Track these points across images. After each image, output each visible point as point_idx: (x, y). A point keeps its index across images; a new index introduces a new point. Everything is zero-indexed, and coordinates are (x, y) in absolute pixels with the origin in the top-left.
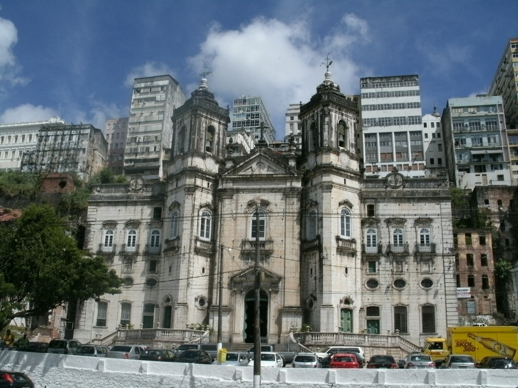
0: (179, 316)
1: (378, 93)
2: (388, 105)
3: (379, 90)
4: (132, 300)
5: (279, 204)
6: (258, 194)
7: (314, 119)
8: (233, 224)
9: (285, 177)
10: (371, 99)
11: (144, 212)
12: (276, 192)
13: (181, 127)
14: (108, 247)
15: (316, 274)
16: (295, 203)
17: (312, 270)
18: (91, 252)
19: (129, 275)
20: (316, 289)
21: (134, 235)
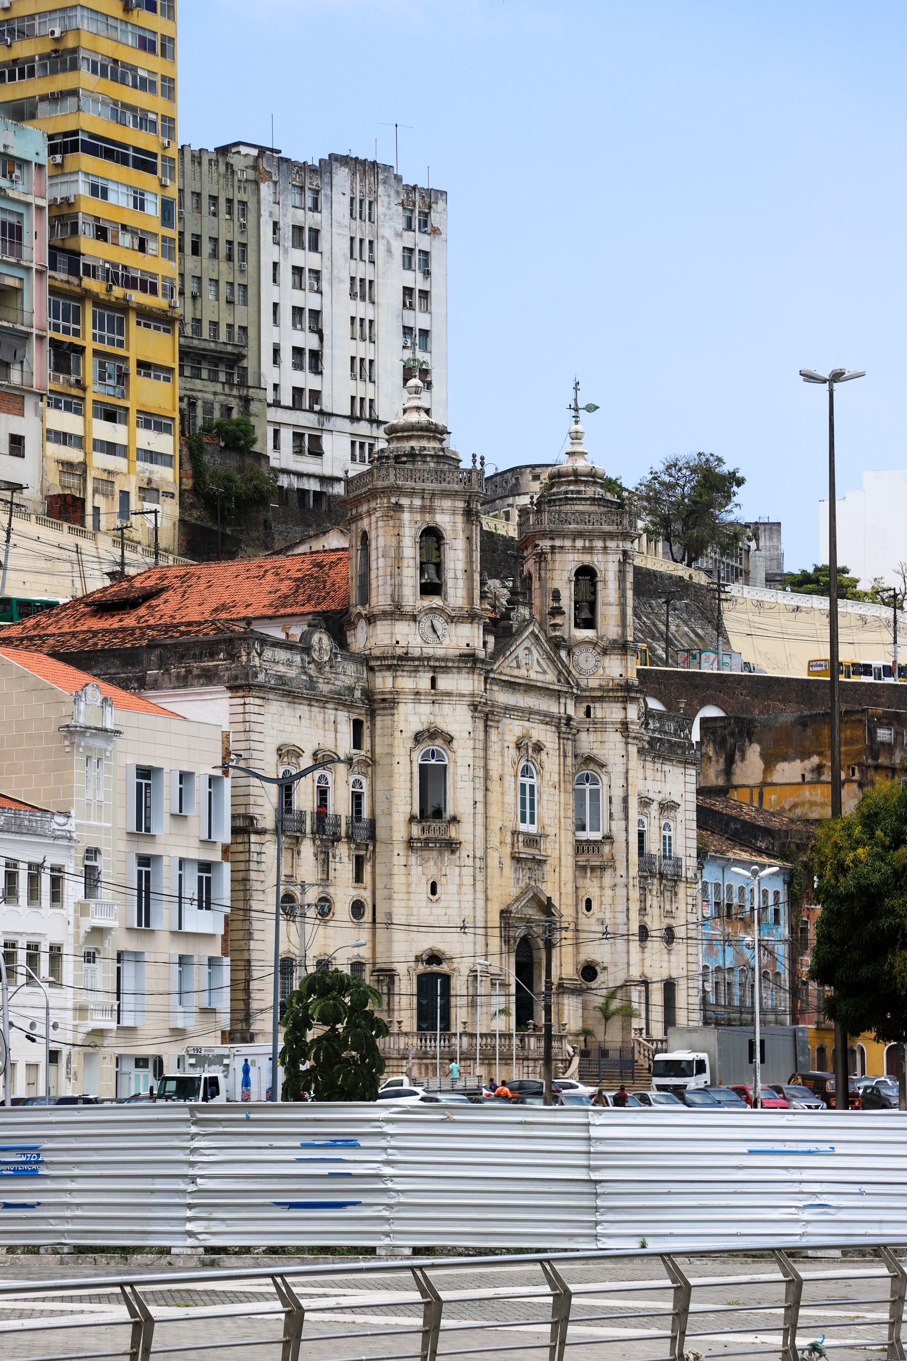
5: (551, 752)
6: (526, 724)
8: (500, 790)
12: (547, 724)
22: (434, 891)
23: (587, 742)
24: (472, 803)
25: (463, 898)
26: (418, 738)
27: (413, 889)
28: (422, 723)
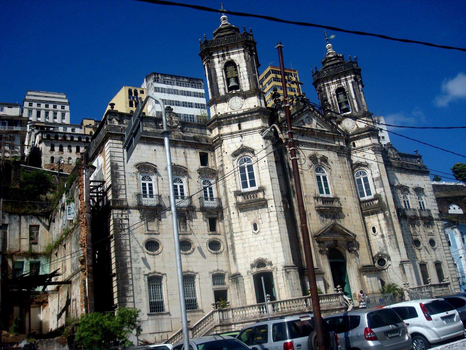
0: (293, 282)
1: (169, 89)
2: (179, 102)
3: (170, 87)
4: (195, 271)
5: (334, 161)
7: (341, 84)
9: (333, 135)
10: (163, 94)
11: (188, 156)
13: (225, 61)
14: (148, 198)
15: (382, 232)
16: (347, 162)
17: (374, 229)
18: (125, 204)
19: (186, 237)
20: (385, 246)
21: (181, 184)
22: (255, 228)
23: (356, 157)
24: (270, 179)
25: (273, 228)
26: (235, 154)
27: (243, 229)
28: (237, 147)
